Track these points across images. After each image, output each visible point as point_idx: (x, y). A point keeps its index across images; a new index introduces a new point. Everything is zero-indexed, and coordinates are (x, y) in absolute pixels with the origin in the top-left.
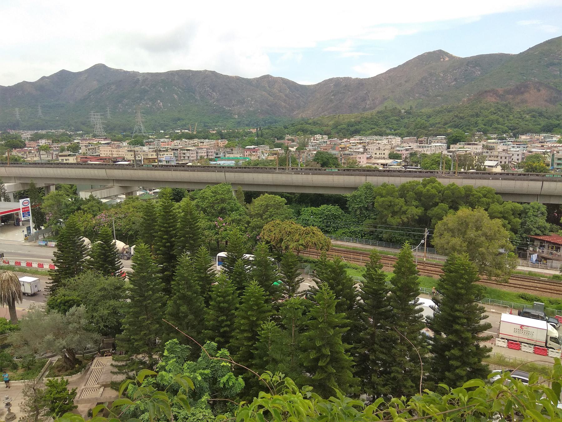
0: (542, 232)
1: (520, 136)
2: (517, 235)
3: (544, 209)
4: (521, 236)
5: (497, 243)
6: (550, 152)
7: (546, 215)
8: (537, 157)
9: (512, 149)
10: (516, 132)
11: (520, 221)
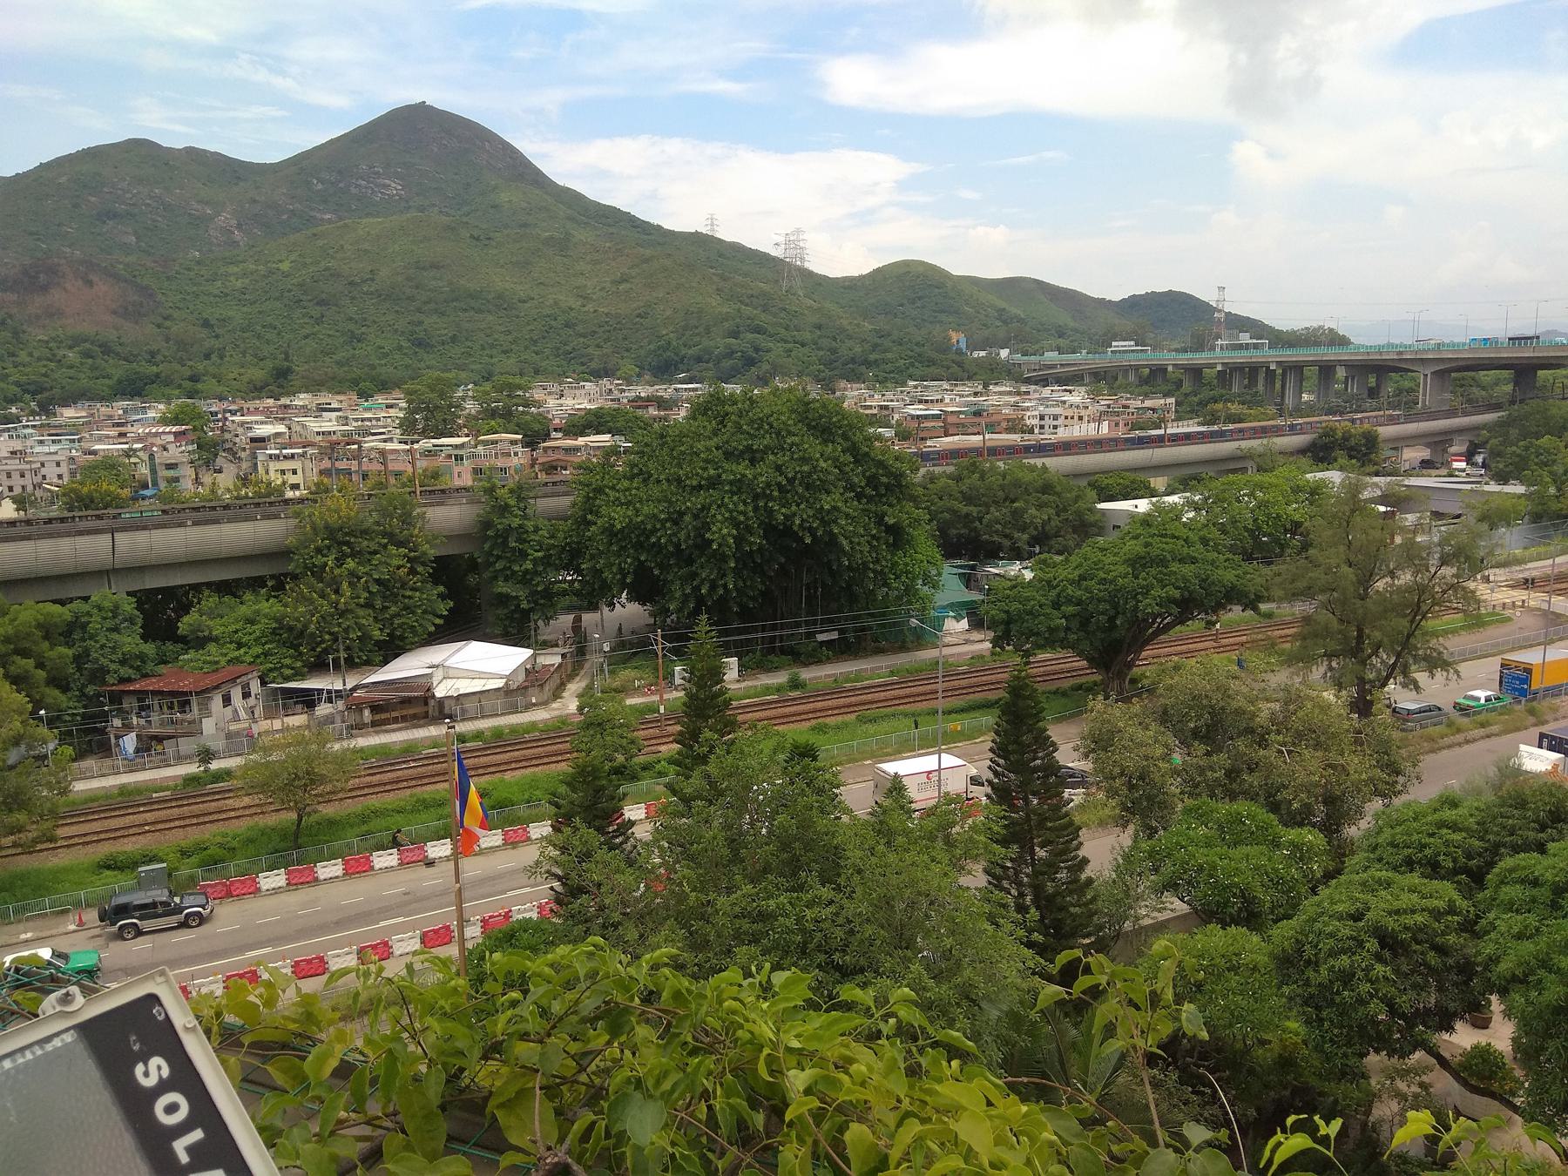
0: (138, 669)
2: (69, 694)
3: (129, 606)
4: (84, 695)
6: (144, 449)
7: (140, 622)
11: (70, 652)
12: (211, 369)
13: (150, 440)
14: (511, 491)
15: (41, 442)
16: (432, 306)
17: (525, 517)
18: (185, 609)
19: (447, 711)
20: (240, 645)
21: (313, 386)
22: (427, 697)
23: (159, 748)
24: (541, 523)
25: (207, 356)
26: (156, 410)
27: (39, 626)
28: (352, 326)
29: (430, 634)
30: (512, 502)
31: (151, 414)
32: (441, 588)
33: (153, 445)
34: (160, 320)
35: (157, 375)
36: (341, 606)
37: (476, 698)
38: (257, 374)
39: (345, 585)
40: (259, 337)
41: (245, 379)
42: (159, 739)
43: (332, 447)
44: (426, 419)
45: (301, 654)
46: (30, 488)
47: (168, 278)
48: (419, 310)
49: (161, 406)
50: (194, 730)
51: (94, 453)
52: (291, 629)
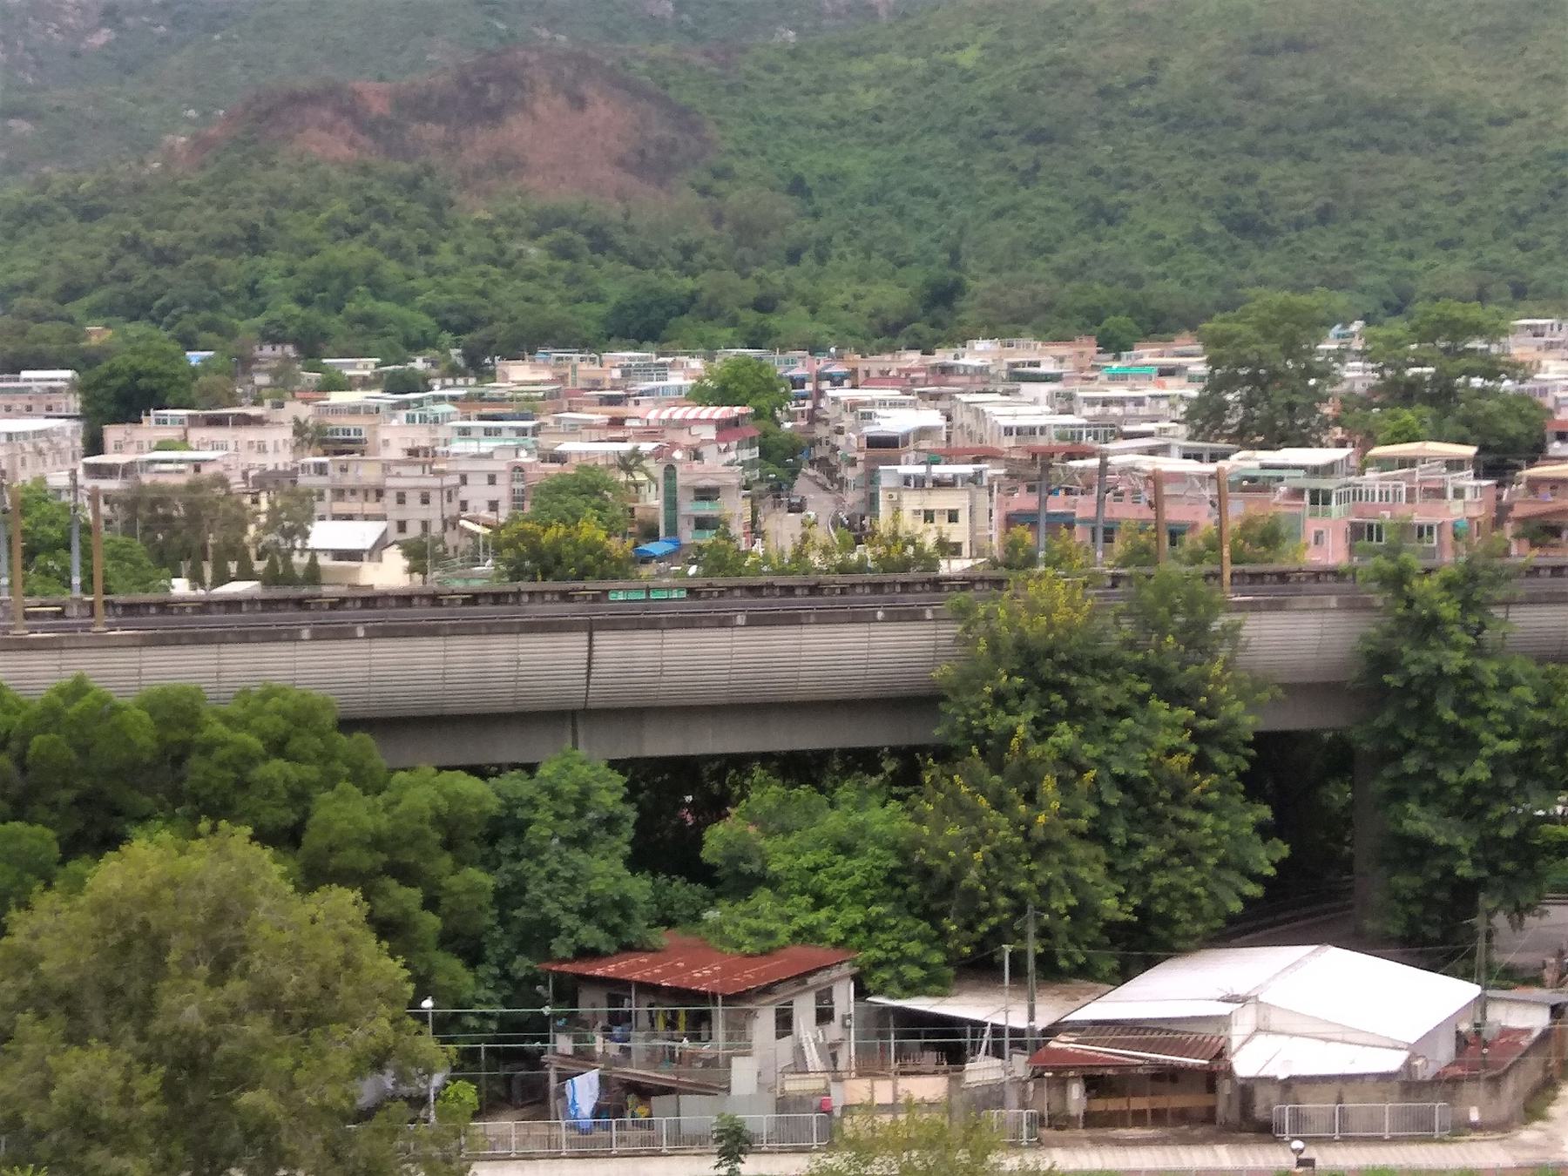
0: (613, 931)
1: (501, 366)
2: (482, 970)
3: (610, 795)
4: (506, 976)
5: (341, 1047)
6: (656, 454)
7: (628, 832)
8: (587, 487)
9: (458, 446)
10: (480, 341)
12: (802, 285)
13: (670, 435)
14: (1449, 585)
15: (465, 432)
16: (1283, 137)
17: (1477, 650)
18: (715, 808)
19: (1259, 1112)
20: (820, 901)
21: (1007, 323)
22: (1213, 1076)
23: (642, 1110)
24: (1517, 668)
25: (794, 257)
26: (687, 371)
27: (439, 820)
28: (1097, 189)
29: (1231, 919)
30: (1449, 610)
31: (676, 379)
32: (1265, 812)
33: (674, 446)
34: (706, 179)
35: (693, 297)
36: (1038, 833)
37: (1331, 1090)
38: (891, 295)
39: (1049, 786)
40: (900, 213)
41: (866, 306)
42: (644, 1092)
43: (1038, 465)
44: (1249, 403)
45: (944, 935)
46: (436, 528)
47: (731, 90)
48: (1250, 150)
49: (696, 364)
50: (714, 1083)
51: (559, 458)
52: (927, 873)
